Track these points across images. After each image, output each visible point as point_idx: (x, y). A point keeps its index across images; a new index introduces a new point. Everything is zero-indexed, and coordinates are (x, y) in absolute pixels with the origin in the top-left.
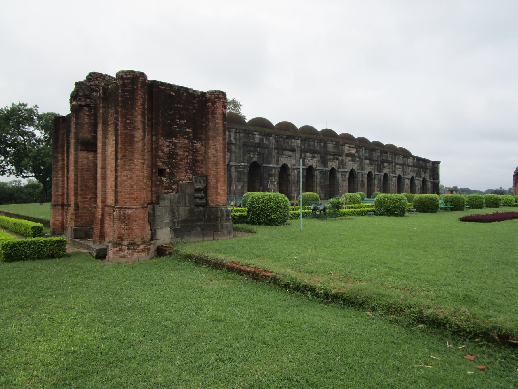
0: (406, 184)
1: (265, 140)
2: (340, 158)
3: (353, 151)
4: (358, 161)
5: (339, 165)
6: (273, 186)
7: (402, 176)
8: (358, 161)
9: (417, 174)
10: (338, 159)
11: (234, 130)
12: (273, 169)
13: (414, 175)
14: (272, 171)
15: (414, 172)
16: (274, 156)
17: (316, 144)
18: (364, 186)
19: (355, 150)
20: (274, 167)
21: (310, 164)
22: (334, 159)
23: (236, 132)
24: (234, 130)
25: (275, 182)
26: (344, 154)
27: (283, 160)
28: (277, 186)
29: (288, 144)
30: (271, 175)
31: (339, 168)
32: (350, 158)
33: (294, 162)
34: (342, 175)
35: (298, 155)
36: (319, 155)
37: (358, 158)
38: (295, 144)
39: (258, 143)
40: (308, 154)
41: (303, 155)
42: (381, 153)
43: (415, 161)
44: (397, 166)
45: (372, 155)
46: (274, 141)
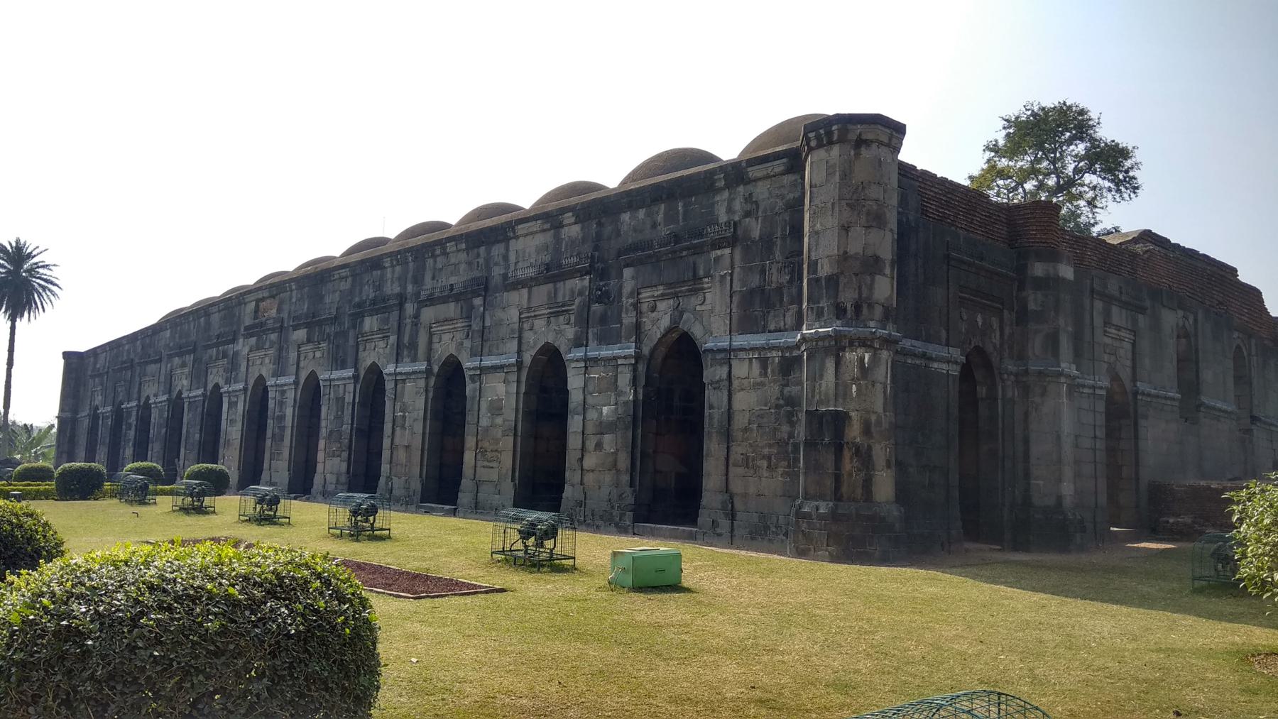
0: (484, 406)
9: (584, 321)
10: (225, 356)
15: (557, 310)
42: (354, 276)
44: (428, 314)
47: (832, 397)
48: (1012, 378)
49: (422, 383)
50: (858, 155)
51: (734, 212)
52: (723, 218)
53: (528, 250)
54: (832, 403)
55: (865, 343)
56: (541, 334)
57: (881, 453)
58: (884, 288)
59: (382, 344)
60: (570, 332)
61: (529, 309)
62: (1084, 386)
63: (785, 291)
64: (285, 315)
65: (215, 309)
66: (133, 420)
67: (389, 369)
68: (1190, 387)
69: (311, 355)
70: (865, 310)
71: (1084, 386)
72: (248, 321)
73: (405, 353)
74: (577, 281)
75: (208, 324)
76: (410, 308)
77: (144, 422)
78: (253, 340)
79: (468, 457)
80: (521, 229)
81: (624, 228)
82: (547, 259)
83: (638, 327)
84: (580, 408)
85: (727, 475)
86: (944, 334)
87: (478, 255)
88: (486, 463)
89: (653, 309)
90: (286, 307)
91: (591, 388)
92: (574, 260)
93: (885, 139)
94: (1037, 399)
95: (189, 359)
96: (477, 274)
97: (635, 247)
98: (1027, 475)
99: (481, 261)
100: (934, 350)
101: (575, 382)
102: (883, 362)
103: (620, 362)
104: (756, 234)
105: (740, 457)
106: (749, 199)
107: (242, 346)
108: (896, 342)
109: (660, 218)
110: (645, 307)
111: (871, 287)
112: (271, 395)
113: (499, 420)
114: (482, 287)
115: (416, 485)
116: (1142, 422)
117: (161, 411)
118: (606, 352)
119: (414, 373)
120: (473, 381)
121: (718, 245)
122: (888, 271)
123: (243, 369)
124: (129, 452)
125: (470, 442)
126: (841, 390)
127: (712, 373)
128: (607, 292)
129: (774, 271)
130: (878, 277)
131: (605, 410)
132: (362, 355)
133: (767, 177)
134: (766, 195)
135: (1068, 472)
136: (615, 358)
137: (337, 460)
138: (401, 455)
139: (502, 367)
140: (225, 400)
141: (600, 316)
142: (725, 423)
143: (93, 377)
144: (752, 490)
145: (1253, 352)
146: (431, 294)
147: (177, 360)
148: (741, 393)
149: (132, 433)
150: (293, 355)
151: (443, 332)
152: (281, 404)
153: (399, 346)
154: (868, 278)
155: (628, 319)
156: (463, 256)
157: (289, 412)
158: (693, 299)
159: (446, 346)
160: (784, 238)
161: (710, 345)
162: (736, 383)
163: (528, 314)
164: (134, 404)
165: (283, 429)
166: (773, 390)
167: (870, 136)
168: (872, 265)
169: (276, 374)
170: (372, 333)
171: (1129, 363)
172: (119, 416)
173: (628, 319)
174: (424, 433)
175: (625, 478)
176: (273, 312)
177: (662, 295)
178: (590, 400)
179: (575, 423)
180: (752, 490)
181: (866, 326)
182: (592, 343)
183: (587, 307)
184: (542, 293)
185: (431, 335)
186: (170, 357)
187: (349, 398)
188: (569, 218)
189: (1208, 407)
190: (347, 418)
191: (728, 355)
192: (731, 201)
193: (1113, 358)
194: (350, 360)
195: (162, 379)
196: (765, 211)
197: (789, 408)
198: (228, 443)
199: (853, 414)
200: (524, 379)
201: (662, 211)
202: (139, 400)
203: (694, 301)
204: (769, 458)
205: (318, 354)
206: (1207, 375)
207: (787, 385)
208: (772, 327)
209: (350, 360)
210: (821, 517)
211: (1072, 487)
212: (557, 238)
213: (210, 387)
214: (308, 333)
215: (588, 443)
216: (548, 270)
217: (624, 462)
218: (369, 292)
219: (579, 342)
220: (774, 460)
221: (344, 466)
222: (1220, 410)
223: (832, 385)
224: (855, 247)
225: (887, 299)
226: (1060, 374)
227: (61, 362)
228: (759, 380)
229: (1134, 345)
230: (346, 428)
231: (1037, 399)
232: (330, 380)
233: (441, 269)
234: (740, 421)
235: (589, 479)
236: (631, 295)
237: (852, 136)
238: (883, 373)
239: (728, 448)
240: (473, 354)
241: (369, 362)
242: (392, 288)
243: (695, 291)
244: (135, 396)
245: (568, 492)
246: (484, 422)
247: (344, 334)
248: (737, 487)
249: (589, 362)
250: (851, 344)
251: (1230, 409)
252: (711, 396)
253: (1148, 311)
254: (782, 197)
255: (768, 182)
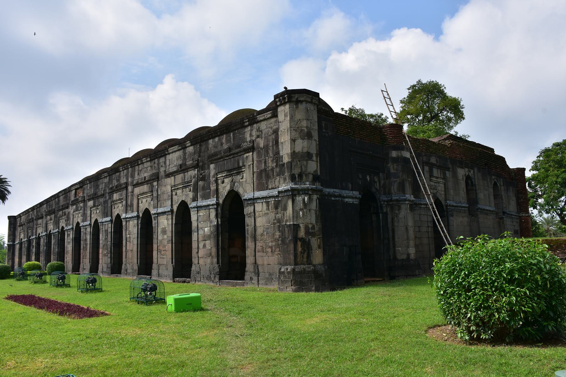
0: (160, 230)
2: (66, 211)
9: (195, 190)
10: (65, 215)
15: (185, 185)
18: (86, 250)
43: (190, 149)
44: (137, 190)
47: (292, 218)
48: (386, 203)
49: (136, 222)
50: (297, 107)
51: (253, 136)
52: (248, 139)
53: (174, 159)
54: (292, 220)
55: (305, 192)
57: (315, 242)
58: (313, 166)
59: (120, 205)
60: (191, 195)
61: (175, 186)
62: (421, 204)
63: (275, 170)
64: (85, 195)
65: (61, 194)
66: (34, 244)
67: (123, 216)
68: (472, 201)
69: (95, 212)
70: (304, 178)
71: (421, 204)
72: (72, 198)
74: (193, 171)
75: (59, 201)
76: (130, 188)
77: (38, 244)
78: (75, 206)
79: (155, 253)
80: (171, 150)
81: (210, 146)
82: (180, 162)
83: (217, 190)
84: (196, 230)
85: (255, 256)
86: (350, 185)
87: (155, 163)
88: (162, 256)
89: (223, 182)
90: (86, 191)
91: (200, 220)
92: (191, 162)
93: (309, 100)
94: (397, 212)
95: (53, 216)
96: (154, 171)
97: (215, 154)
98: (394, 246)
99: (156, 165)
100: (345, 193)
101: (194, 217)
102: (314, 200)
103: (211, 207)
104: (262, 145)
105: (260, 248)
106: (259, 130)
107: (71, 209)
108: (321, 191)
109: (224, 141)
110: (220, 181)
111: (306, 167)
112: (82, 230)
113: (165, 237)
114: (156, 177)
115: (136, 267)
116: (451, 218)
117: (44, 239)
118: (205, 203)
119: (132, 217)
120: (155, 220)
121: (247, 150)
122: (314, 158)
123: (72, 220)
124: (33, 258)
125: (155, 246)
126: (295, 215)
127: (248, 210)
128: (204, 175)
129: (270, 161)
130: (309, 162)
131: (206, 229)
132: (113, 210)
133: (265, 120)
134: (265, 127)
135: (412, 243)
136: (209, 205)
137: (106, 258)
138: (130, 255)
140: (66, 233)
141: (201, 188)
142: (253, 232)
143: (20, 226)
144: (266, 263)
145: (502, 184)
146: (138, 182)
147: (48, 217)
148: (260, 218)
149: (34, 250)
150: (89, 212)
152: (86, 234)
153: (127, 205)
154: (305, 163)
155: (213, 187)
156: (149, 164)
157: (88, 237)
158: (238, 176)
159: (145, 204)
160: (273, 146)
161: (245, 198)
162: (257, 214)
163: (174, 188)
164: (34, 237)
165: (86, 244)
166: (272, 216)
167: (302, 99)
168: (308, 156)
169: (83, 221)
170: (117, 200)
171: (443, 193)
172: (29, 241)
173: (213, 187)
174: (138, 244)
175: (215, 260)
176: (81, 195)
177: (226, 175)
178: (200, 226)
179: (194, 236)
180: (266, 263)
181: (305, 184)
182: (199, 200)
183: (196, 184)
184: (179, 177)
185: (138, 200)
186: (46, 215)
187: (109, 230)
189: (481, 209)
190: (109, 239)
191: (254, 200)
192: (251, 130)
193: (435, 191)
194: (109, 213)
195: (44, 226)
196: (265, 135)
197: (278, 224)
198: (68, 252)
199: (301, 225)
200: (174, 218)
201: (224, 138)
202: (36, 235)
203: (239, 177)
204: (271, 247)
205: (98, 211)
206: (481, 196)
207: (277, 214)
208: (270, 187)
209: (109, 213)
210: (288, 273)
211: (414, 249)
212: (185, 154)
213: (60, 228)
214: (94, 203)
215: (200, 245)
216: (181, 167)
217: (214, 250)
218: (115, 183)
219: (195, 199)
220: (273, 248)
221: (109, 260)
222: (487, 210)
223: (291, 212)
224: (298, 149)
225: (314, 172)
226: (405, 200)
227: (7, 221)
228: (266, 212)
229: (445, 184)
230: (109, 243)
231: (397, 212)
232: (103, 222)
234: (259, 231)
235: (201, 261)
236: (214, 176)
237: (294, 99)
238: (314, 205)
239: (255, 244)
240: (154, 208)
241: (116, 214)
242: (123, 180)
243: (238, 173)
244: (35, 234)
245: (193, 268)
246: (160, 238)
247: (106, 202)
248: (259, 262)
249: (198, 208)
250: (299, 194)
251: (492, 209)
252: (249, 221)
253: (451, 170)
254: (271, 128)
255: (265, 122)
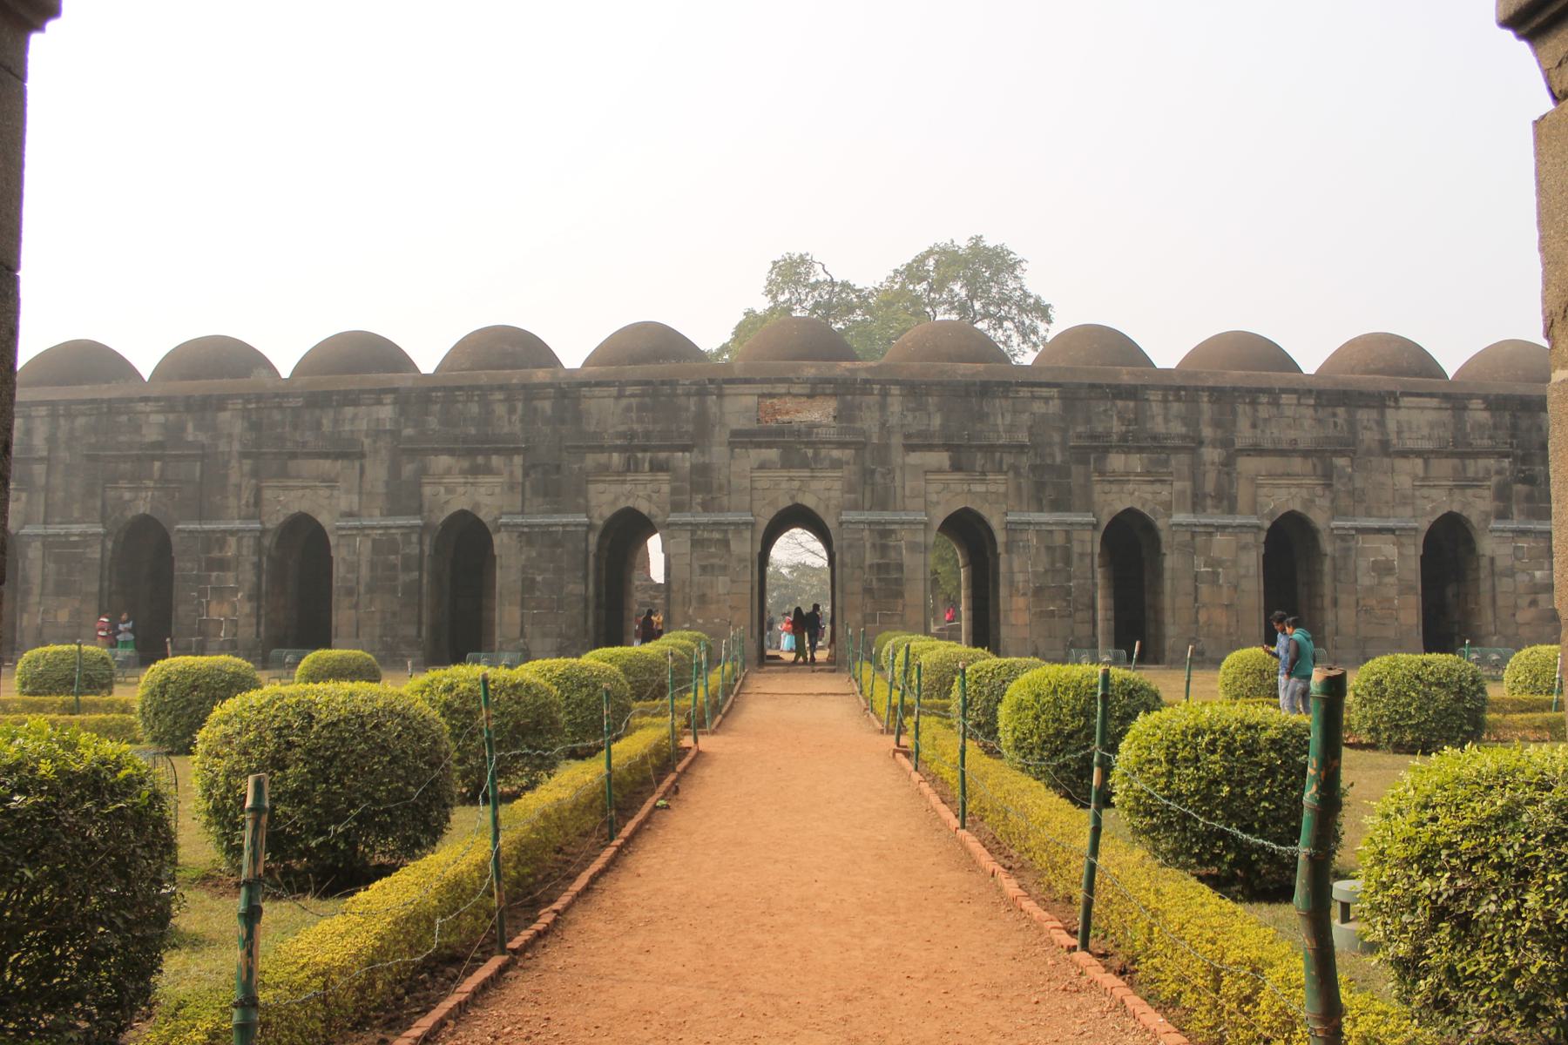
0: (1363, 564)
1: (190, 427)
2: (684, 460)
3: (818, 413)
4: (836, 464)
5: (674, 491)
6: (226, 609)
7: (1319, 517)
8: (836, 464)
10: (656, 467)
11: (43, 411)
12: (232, 541)
13: (1477, 506)
14: (222, 544)
15: (1464, 483)
16: (239, 486)
17: (500, 410)
19: (831, 405)
20: (233, 533)
21: (459, 503)
22: (631, 467)
23: (54, 415)
24: (43, 411)
25: (235, 591)
26: (721, 435)
27: (284, 502)
28: (247, 608)
29: (319, 425)
30: (222, 565)
31: (677, 507)
32: (773, 454)
33: (346, 501)
34: (696, 543)
35: (377, 472)
36: (518, 460)
37: (842, 445)
38: (363, 425)
39: (154, 445)
40: (444, 461)
41: (408, 469)
44: (1247, 465)
45: (982, 417)
46: (238, 427)
56: (1439, 502)
61: (1423, 479)
73: (1209, 502)
76: (1211, 454)
87: (1334, 415)
96: (1331, 432)
131: (1538, 574)
139: (1391, 531)
151: (1278, 486)
156: (1310, 412)
163: (1425, 481)
178: (1517, 564)
184: (1443, 467)
188: (1476, 404)
233: (1265, 420)
246: (1366, 580)
